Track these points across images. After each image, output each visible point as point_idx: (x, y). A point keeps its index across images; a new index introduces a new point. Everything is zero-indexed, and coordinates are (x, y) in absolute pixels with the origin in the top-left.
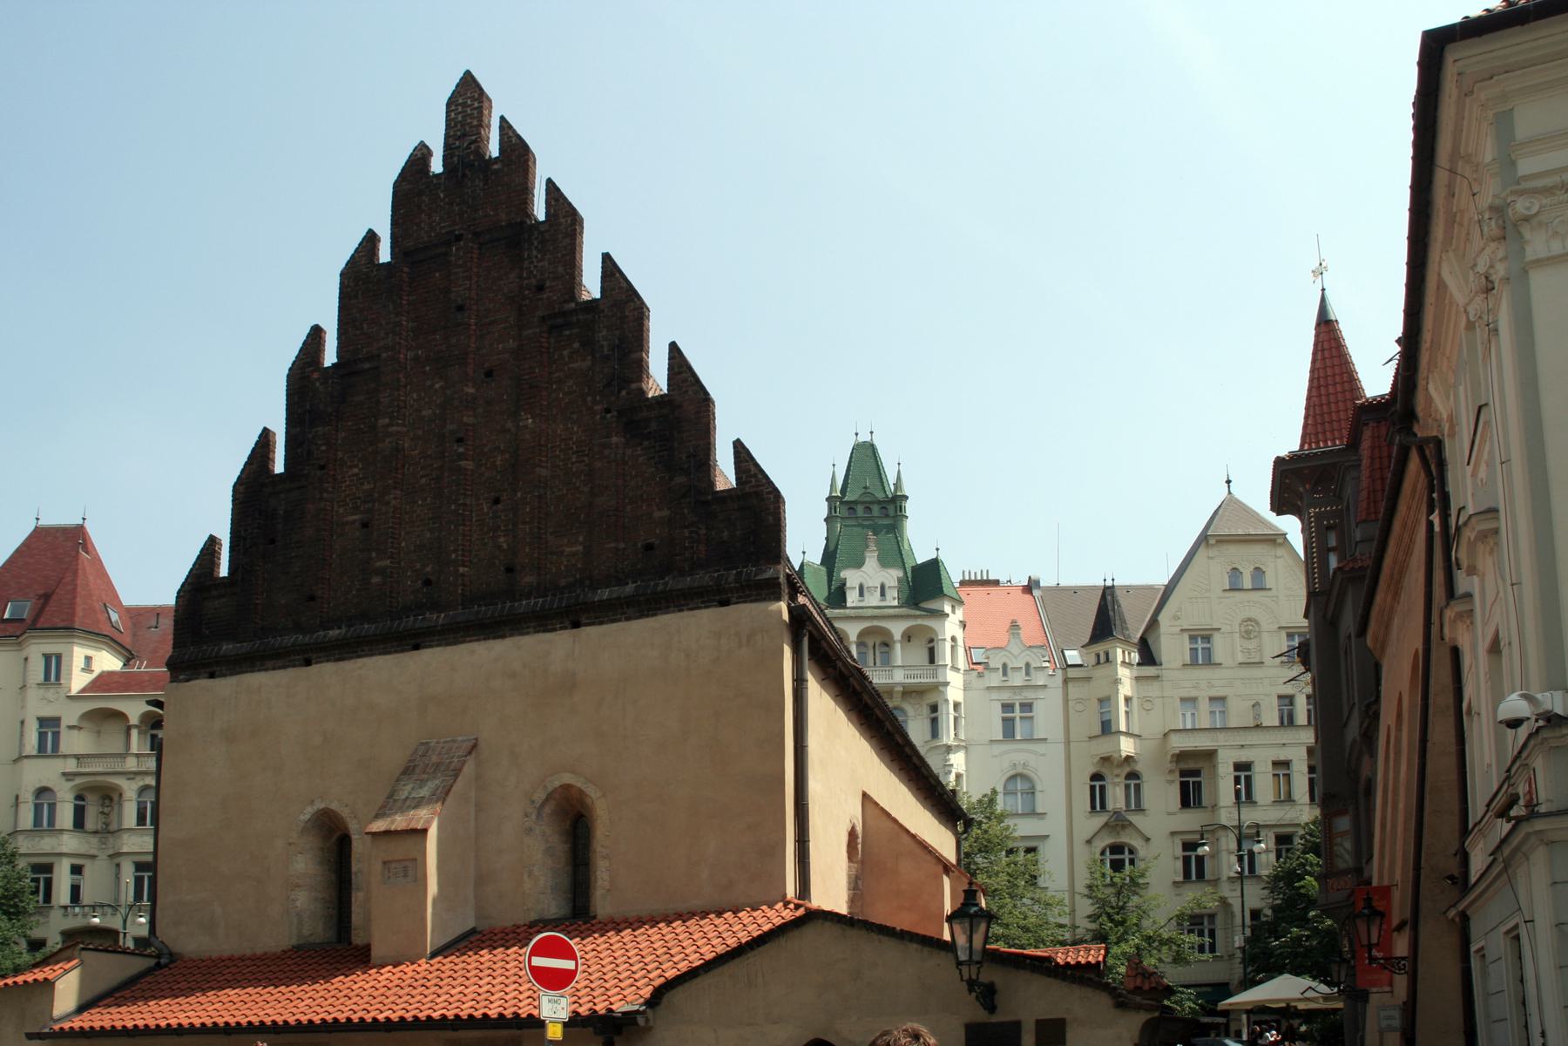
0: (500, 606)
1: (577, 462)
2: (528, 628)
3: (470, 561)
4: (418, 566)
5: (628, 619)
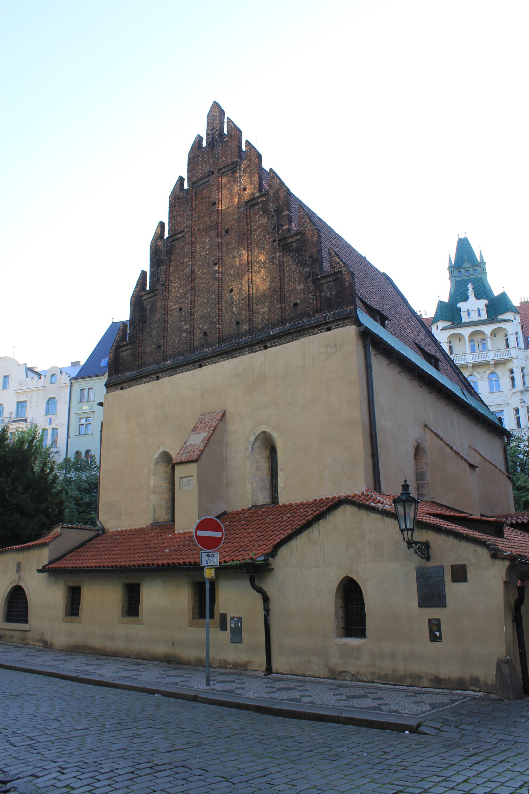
0: (233, 342)
1: (264, 267)
2: (246, 351)
3: (222, 321)
4: (201, 326)
5: (287, 342)
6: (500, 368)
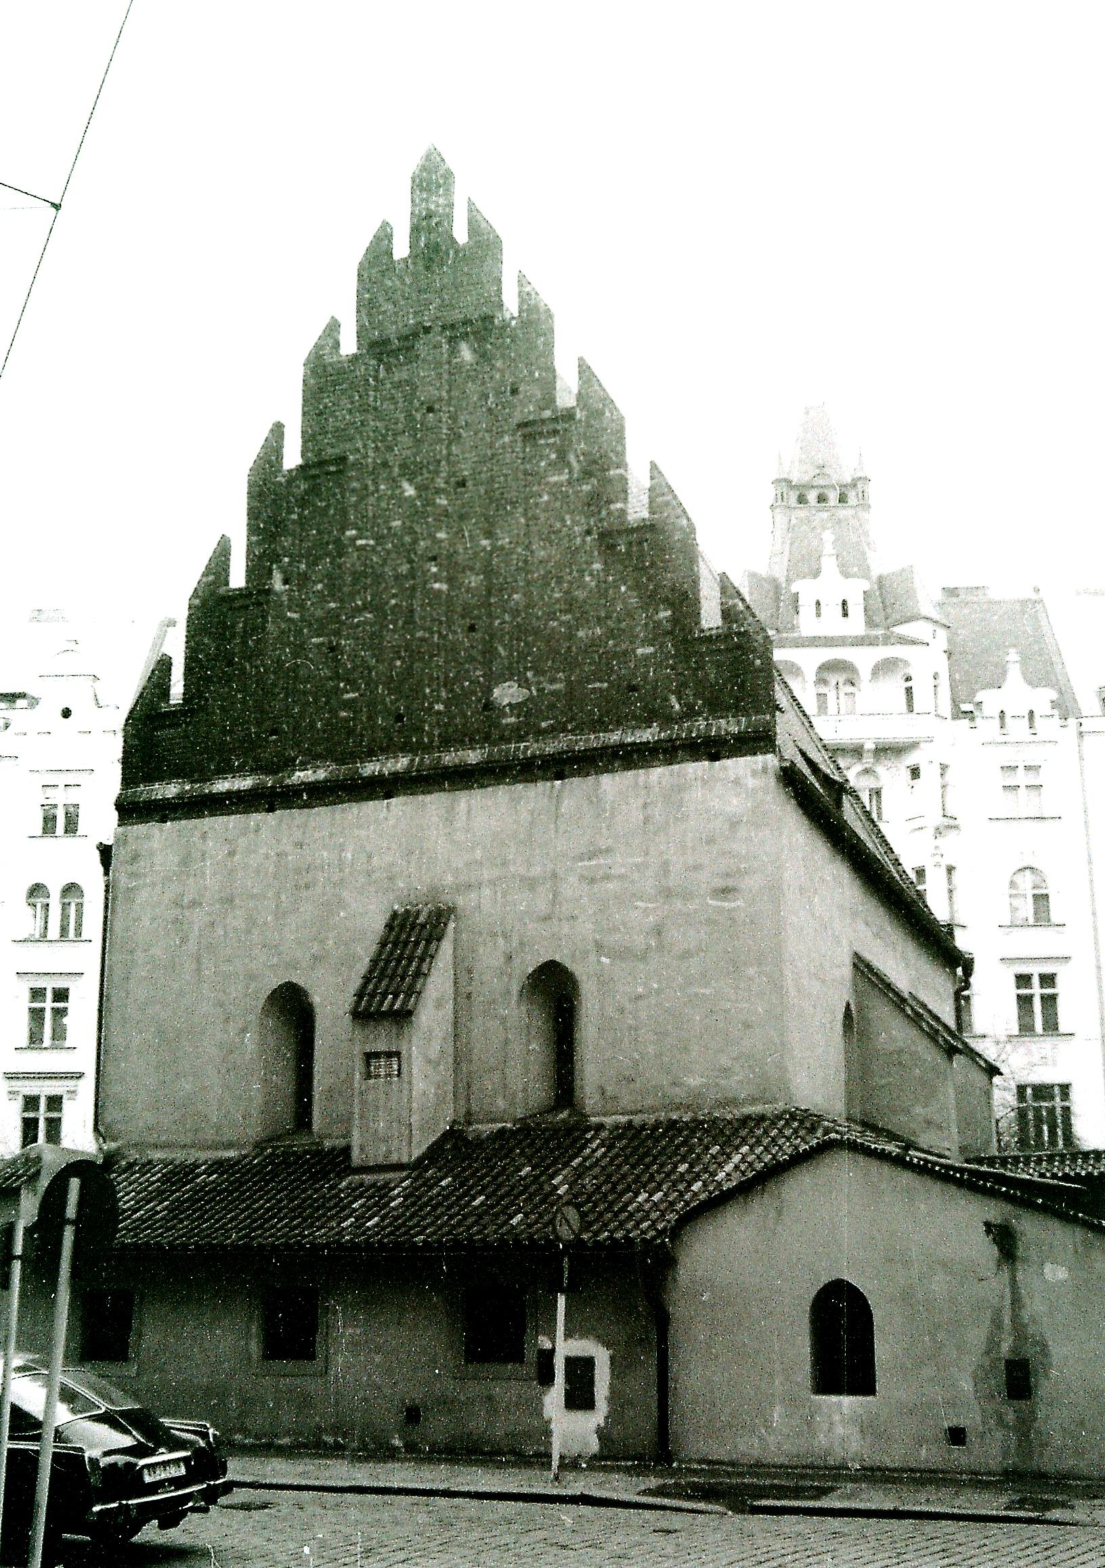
6: (886, 762)
